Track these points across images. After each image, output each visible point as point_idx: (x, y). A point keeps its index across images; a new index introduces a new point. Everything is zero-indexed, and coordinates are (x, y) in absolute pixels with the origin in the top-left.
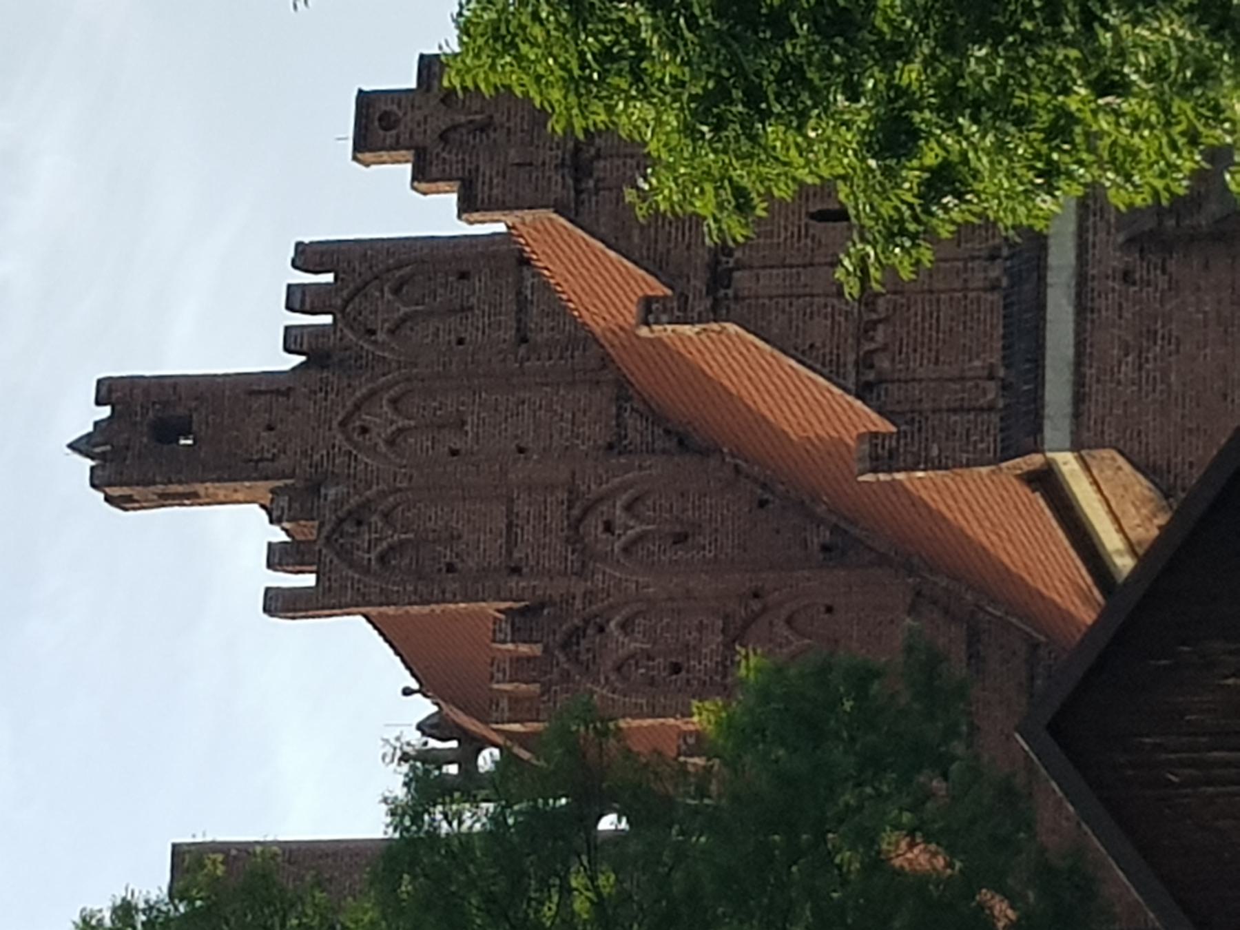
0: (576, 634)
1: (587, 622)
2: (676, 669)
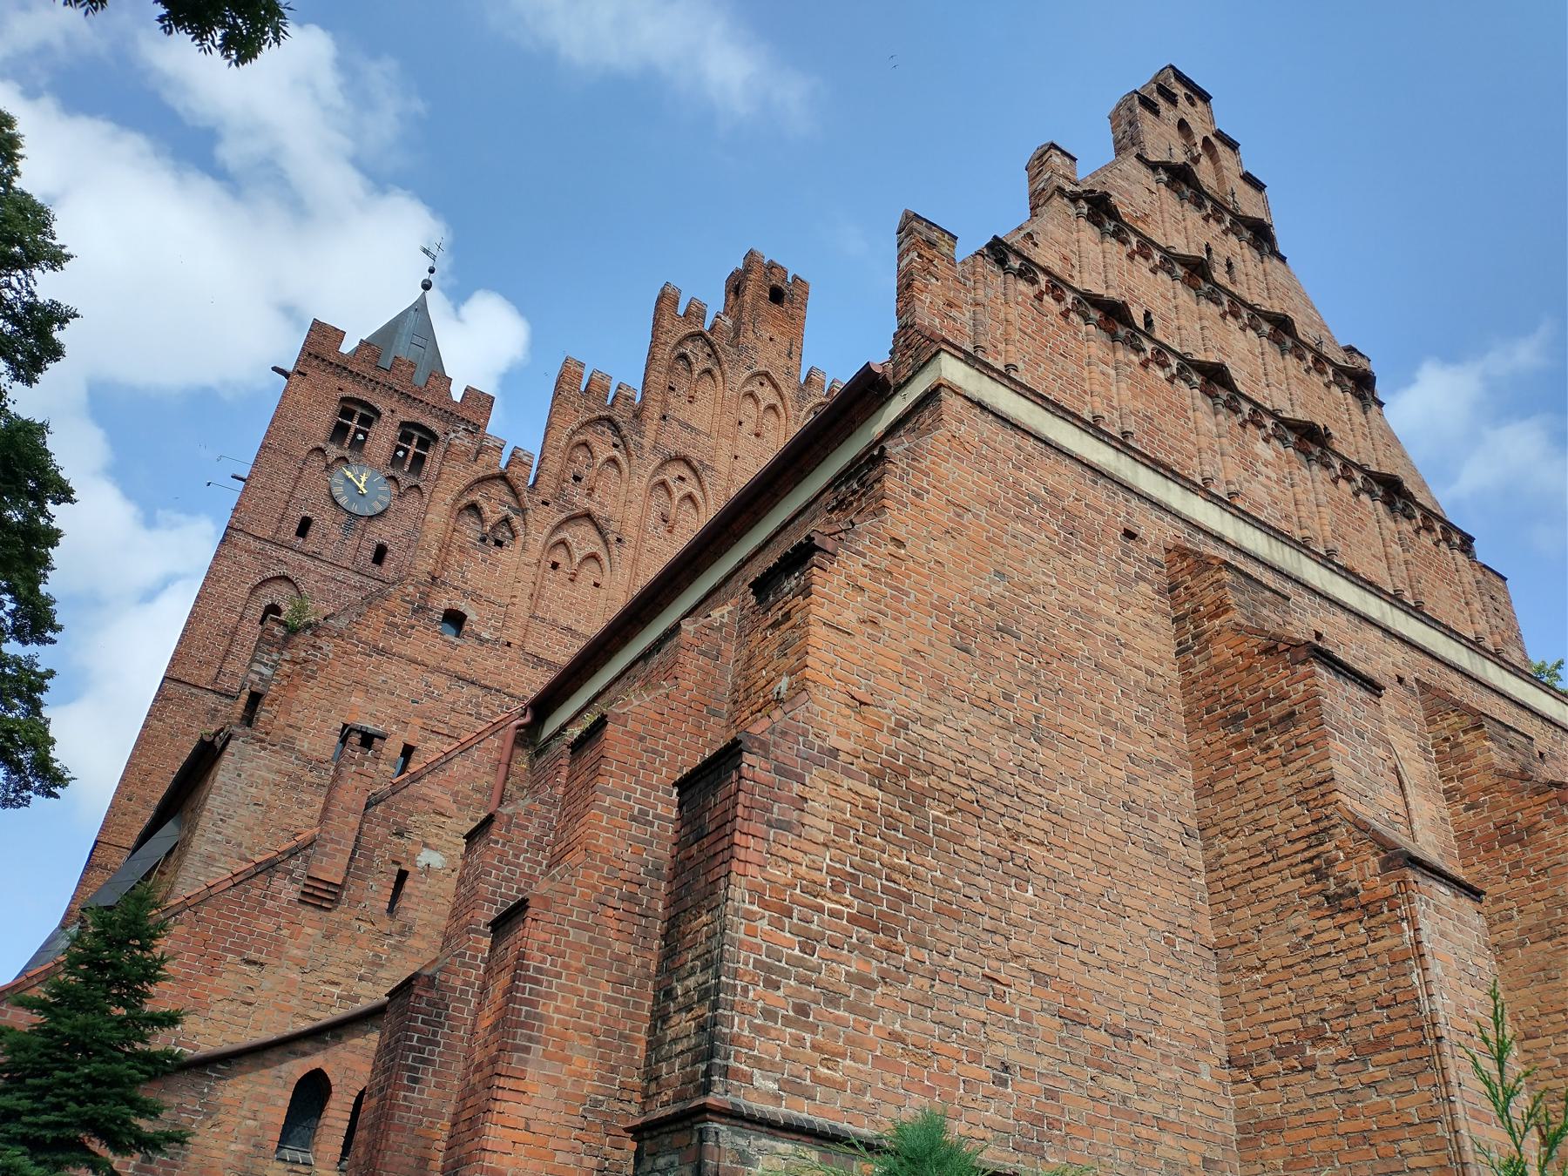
0: (616, 428)
1: (622, 438)
2: (577, 479)
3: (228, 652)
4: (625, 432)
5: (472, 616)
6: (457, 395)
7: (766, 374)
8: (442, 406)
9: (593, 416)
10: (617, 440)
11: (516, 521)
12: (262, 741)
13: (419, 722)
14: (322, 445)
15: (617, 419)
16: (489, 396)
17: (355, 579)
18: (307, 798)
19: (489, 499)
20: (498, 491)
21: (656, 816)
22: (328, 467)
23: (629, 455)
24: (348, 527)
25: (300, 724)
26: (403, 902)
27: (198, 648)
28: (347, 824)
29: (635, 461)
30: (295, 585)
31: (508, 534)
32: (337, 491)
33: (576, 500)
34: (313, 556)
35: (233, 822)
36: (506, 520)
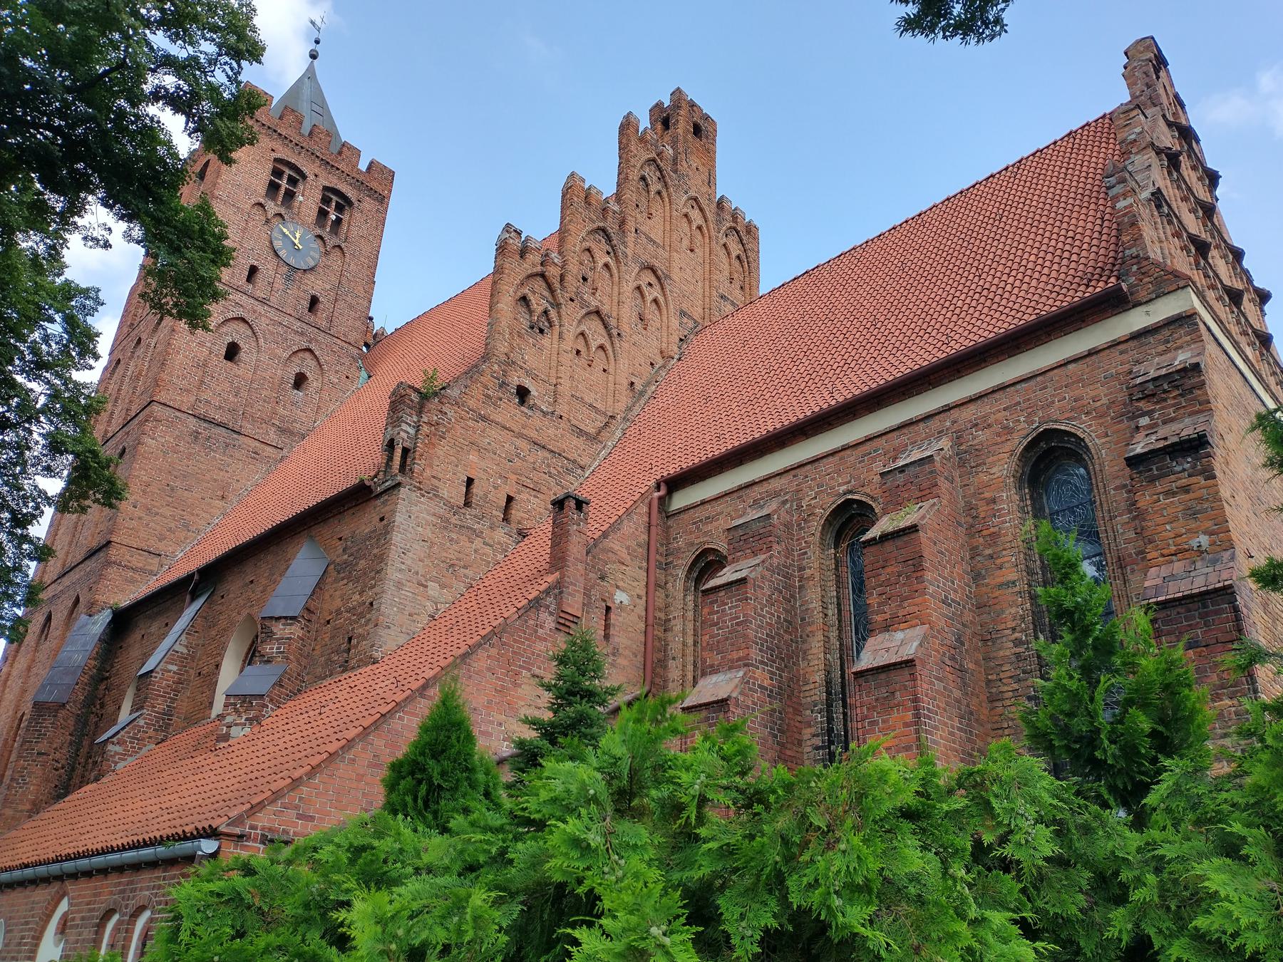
2: (585, 279)
3: (202, 382)
4: (615, 242)
5: (534, 393)
6: (363, 166)
7: (695, 199)
8: (354, 175)
9: (595, 226)
10: (610, 250)
11: (553, 314)
12: (421, 489)
13: (514, 477)
14: (262, 200)
15: (610, 230)
16: (390, 171)
17: (297, 325)
18: (454, 536)
19: (534, 293)
20: (539, 284)
21: (952, 600)
22: (268, 221)
23: (618, 261)
24: (288, 278)
25: (440, 476)
26: (612, 632)
27: (178, 377)
28: (578, 570)
29: (623, 268)
30: (250, 326)
31: (546, 324)
32: (278, 244)
33: (585, 297)
34: (263, 302)
35: (410, 554)
36: (546, 312)
